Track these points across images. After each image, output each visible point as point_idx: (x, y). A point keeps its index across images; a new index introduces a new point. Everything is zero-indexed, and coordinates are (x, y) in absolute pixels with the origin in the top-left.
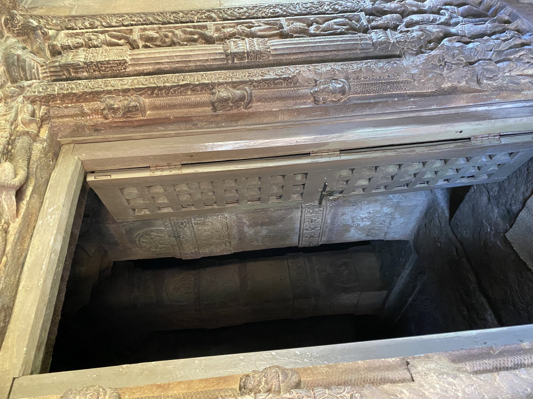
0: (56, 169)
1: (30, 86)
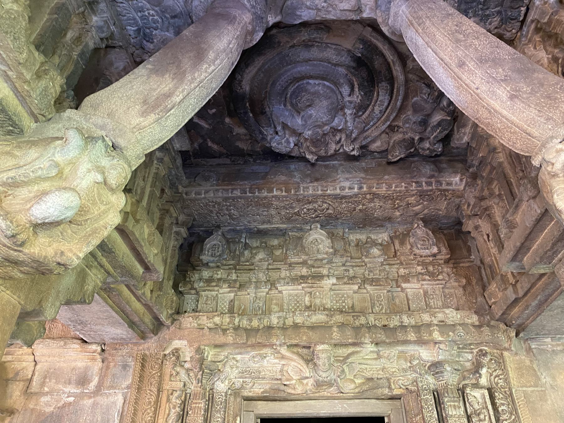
0: (378, 402)
1: (427, 379)
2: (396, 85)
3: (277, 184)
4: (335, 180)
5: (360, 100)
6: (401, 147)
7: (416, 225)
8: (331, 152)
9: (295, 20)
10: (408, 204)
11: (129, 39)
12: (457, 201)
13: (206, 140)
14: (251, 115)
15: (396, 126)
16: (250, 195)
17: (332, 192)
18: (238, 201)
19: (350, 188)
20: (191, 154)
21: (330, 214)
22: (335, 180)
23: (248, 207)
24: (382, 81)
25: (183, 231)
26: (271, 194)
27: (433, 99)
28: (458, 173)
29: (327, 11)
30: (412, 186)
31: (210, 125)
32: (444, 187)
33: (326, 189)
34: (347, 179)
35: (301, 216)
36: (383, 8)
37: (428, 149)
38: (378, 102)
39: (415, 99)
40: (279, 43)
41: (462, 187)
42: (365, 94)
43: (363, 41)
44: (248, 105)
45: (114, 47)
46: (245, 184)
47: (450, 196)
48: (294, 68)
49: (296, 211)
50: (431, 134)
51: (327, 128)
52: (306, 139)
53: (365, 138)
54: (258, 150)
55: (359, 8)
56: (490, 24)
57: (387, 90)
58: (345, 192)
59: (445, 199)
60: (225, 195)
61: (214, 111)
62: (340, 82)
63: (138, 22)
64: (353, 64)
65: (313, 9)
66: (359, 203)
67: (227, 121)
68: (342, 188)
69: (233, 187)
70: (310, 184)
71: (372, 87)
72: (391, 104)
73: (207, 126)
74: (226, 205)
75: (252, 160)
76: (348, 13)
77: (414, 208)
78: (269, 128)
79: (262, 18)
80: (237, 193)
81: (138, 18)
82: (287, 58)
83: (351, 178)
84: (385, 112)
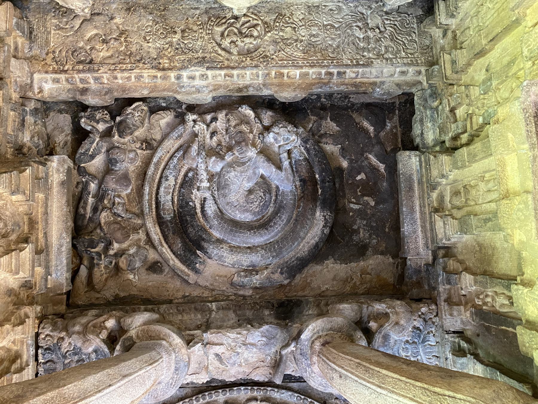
2: (154, 213)
3: (293, 84)
4: (214, 90)
5: (192, 193)
6: (134, 125)
7: (86, 11)
8: (221, 116)
9: (267, 331)
10: (104, 41)
11: (436, 331)
12: (36, 51)
13: (375, 136)
14: (317, 176)
15: (144, 150)
16: (332, 70)
17: (218, 72)
18: (352, 62)
19: (192, 78)
20: (397, 111)
21: (218, 25)
22: (214, 90)
23: (338, 47)
24: (170, 221)
25: (442, 17)
26: (304, 70)
27: (108, 195)
28: (48, 97)
29: (236, 342)
30: (108, 80)
31: (367, 158)
32: (63, 76)
33: (227, 77)
34: (198, 91)
35: (262, 20)
36: (182, 364)
37: (98, 122)
38: (171, 191)
39: (129, 191)
40: (282, 273)
41: (36, 76)
42: (187, 203)
43: (197, 272)
44: (320, 191)
45: (454, 332)
46: (337, 85)
47: (49, 61)
48: (268, 240)
49: (269, 34)
50: (100, 144)
51: (229, 158)
52: (254, 145)
53: (180, 136)
54: (312, 117)
55: (205, 346)
56: (70, 343)
57: (164, 209)
58: (200, 72)
59: (54, 52)
60: (367, 70)
61: (359, 178)
62: (218, 221)
63: (423, 350)
64: (205, 245)
65: (249, 344)
66: (179, 50)
67: (346, 163)
68: (203, 77)
69: (354, 80)
70: (248, 83)
71: (181, 213)
72: (155, 186)
73: (370, 156)
74: (369, 51)
75: (323, 100)
76: (216, 341)
77: (95, 32)
78: (297, 158)
79: (301, 354)
80: (350, 73)
81: (422, 354)
82: (275, 254)
83: (193, 93)
84: (161, 177)
